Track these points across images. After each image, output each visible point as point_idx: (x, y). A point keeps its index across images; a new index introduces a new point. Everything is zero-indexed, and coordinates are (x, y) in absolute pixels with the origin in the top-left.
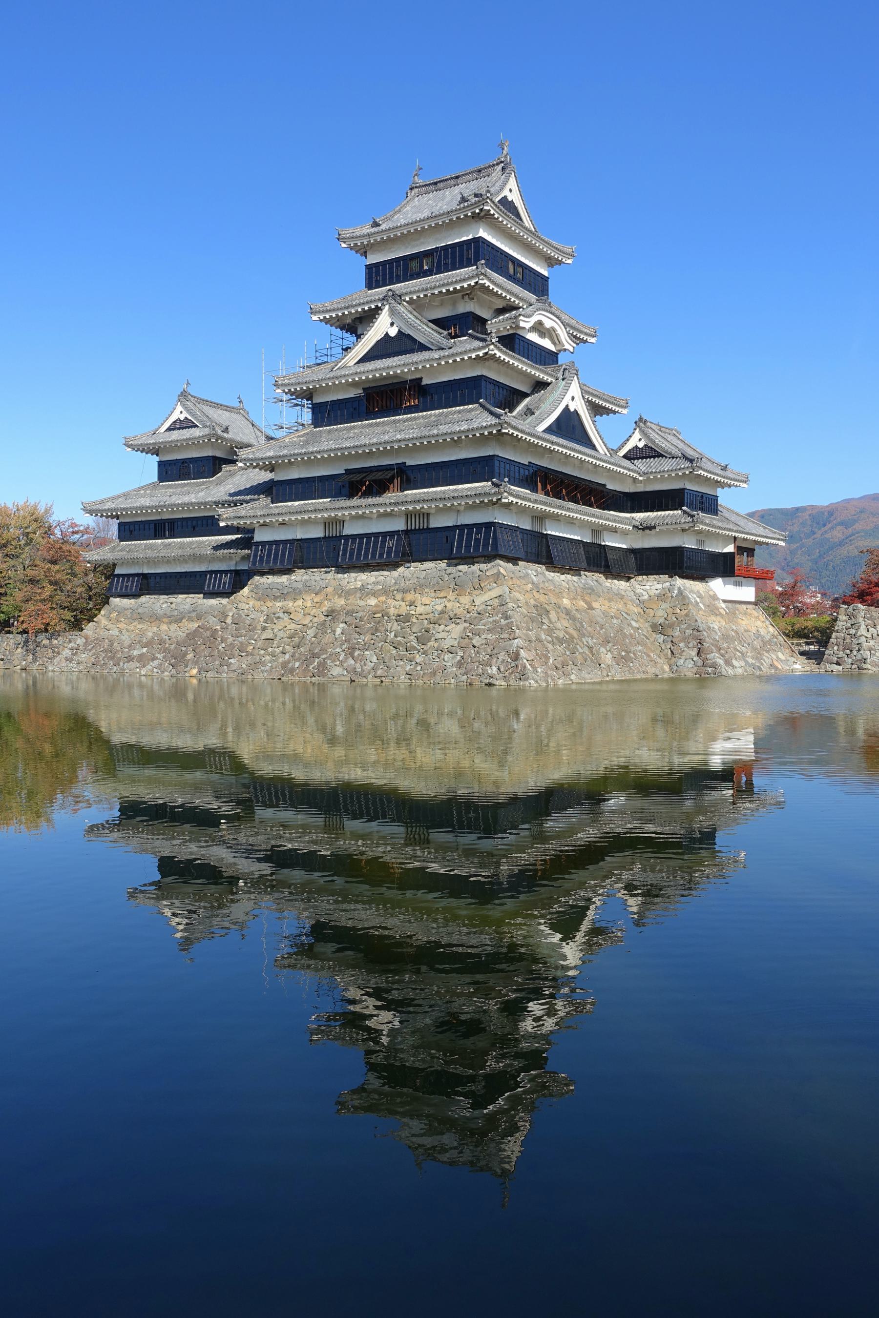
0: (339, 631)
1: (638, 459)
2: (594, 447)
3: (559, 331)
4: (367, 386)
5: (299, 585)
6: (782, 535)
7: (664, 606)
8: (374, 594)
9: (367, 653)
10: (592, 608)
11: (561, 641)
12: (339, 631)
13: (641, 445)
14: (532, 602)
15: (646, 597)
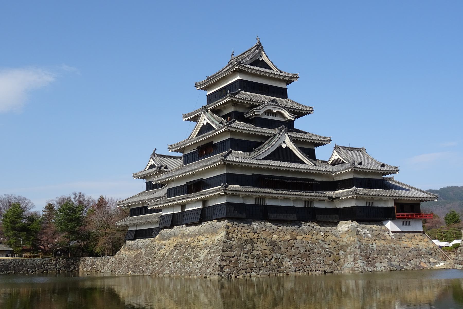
0: (175, 253)
1: (336, 165)
2: (303, 163)
3: (283, 112)
4: (198, 145)
5: (172, 233)
6: (435, 196)
7: (347, 236)
8: (191, 237)
9: (178, 263)
10: (296, 239)
11: (253, 256)
12: (175, 253)
13: (336, 159)
14: (246, 238)
15: (341, 232)
